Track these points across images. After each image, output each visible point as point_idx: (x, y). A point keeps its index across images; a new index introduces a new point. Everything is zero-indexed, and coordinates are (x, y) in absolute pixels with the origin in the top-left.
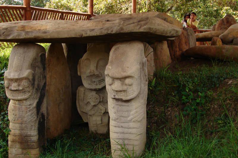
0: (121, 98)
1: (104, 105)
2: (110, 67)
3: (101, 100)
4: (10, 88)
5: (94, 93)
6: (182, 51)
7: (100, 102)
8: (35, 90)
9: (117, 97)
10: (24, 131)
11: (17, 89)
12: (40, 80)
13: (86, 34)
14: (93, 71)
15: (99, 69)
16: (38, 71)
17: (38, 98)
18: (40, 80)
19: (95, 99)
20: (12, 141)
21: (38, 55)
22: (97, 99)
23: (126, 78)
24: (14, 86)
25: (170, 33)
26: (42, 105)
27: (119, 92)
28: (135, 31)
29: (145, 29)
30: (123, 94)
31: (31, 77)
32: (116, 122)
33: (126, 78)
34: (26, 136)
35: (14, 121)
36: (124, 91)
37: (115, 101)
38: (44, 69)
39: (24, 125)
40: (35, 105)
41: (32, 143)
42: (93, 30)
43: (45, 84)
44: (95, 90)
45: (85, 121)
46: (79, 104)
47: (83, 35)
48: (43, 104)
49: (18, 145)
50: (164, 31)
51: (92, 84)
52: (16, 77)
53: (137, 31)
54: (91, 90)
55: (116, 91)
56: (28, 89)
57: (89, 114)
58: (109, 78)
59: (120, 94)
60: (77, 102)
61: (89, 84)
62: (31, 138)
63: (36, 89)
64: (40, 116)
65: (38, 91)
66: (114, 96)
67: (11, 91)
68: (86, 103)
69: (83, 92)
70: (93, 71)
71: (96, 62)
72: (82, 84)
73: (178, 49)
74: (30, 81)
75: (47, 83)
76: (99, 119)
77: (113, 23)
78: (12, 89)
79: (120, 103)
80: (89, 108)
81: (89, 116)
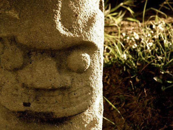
9: (34, 107)
27: (46, 94)
30: (60, 97)
36: (64, 89)
55: (37, 90)
59: (46, 98)
66: (25, 104)
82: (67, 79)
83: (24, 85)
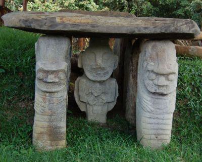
2: (152, 63)
4: (45, 80)
5: (98, 85)
7: (102, 93)
9: (157, 91)
13: (139, 31)
20: (39, 132)
22: (100, 90)
24: (51, 78)
31: (66, 70)
32: (152, 115)
42: (146, 28)
46: (79, 96)
52: (54, 69)
53: (188, 32)
55: (159, 86)
74: (65, 73)
77: (165, 23)
78: (48, 81)
79: (157, 96)
83: (155, 85)
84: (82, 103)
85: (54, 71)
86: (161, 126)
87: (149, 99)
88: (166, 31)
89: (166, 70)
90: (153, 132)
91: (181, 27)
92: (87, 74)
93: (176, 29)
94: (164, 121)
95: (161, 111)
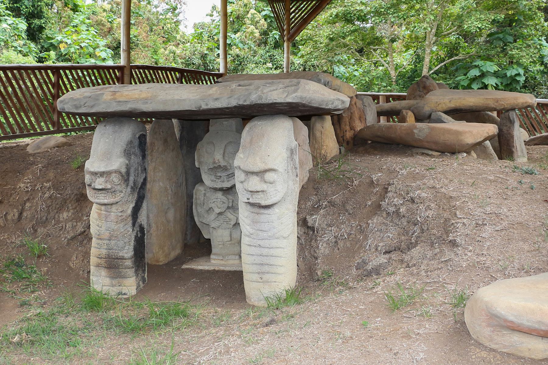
0: (258, 202)
1: (234, 213)
3: (230, 205)
5: (220, 195)
6: (354, 130)
7: (228, 208)
8: (129, 189)
9: (251, 201)
10: (114, 251)
11: (103, 187)
12: (138, 174)
14: (218, 160)
15: (226, 158)
16: (136, 160)
17: (134, 202)
18: (138, 174)
19: (221, 203)
21: (135, 136)
22: (224, 203)
23: (266, 171)
24: (99, 183)
25: (333, 104)
26: (140, 212)
27: (256, 194)
28: (279, 101)
29: (294, 99)
30: (262, 196)
31: (123, 170)
33: (266, 171)
34: (117, 259)
35: (98, 235)
36: (263, 191)
37: (249, 207)
38: (144, 157)
39: (113, 242)
40: (129, 211)
41: (125, 268)
43: (145, 179)
44: (221, 189)
45: (206, 237)
47: (201, 107)
48: (141, 210)
49: (104, 272)
50: (323, 101)
51: (217, 180)
52: (102, 169)
54: (216, 190)
55: (251, 192)
56: (119, 188)
57: (211, 226)
58: (240, 172)
60: (194, 207)
61: (212, 181)
62: (125, 261)
63: (132, 188)
64: (137, 228)
65: (134, 191)
66: (248, 199)
67: (95, 191)
68: (207, 209)
69: (204, 192)
70: (218, 160)
71: (224, 147)
72: (201, 181)
73: (348, 128)
74: (122, 176)
75: (149, 179)
76: (226, 233)
77: (247, 90)
78: (96, 187)
79: (256, 210)
80: (213, 216)
81: (211, 229)
82: (264, 187)
84: (205, 225)
85: (104, 172)
86: (265, 260)
87: (246, 214)
88: (245, 101)
89: (259, 166)
90: (255, 268)
91: (270, 93)
92: (205, 177)
93: (260, 98)
94: (272, 252)
95: (265, 234)
